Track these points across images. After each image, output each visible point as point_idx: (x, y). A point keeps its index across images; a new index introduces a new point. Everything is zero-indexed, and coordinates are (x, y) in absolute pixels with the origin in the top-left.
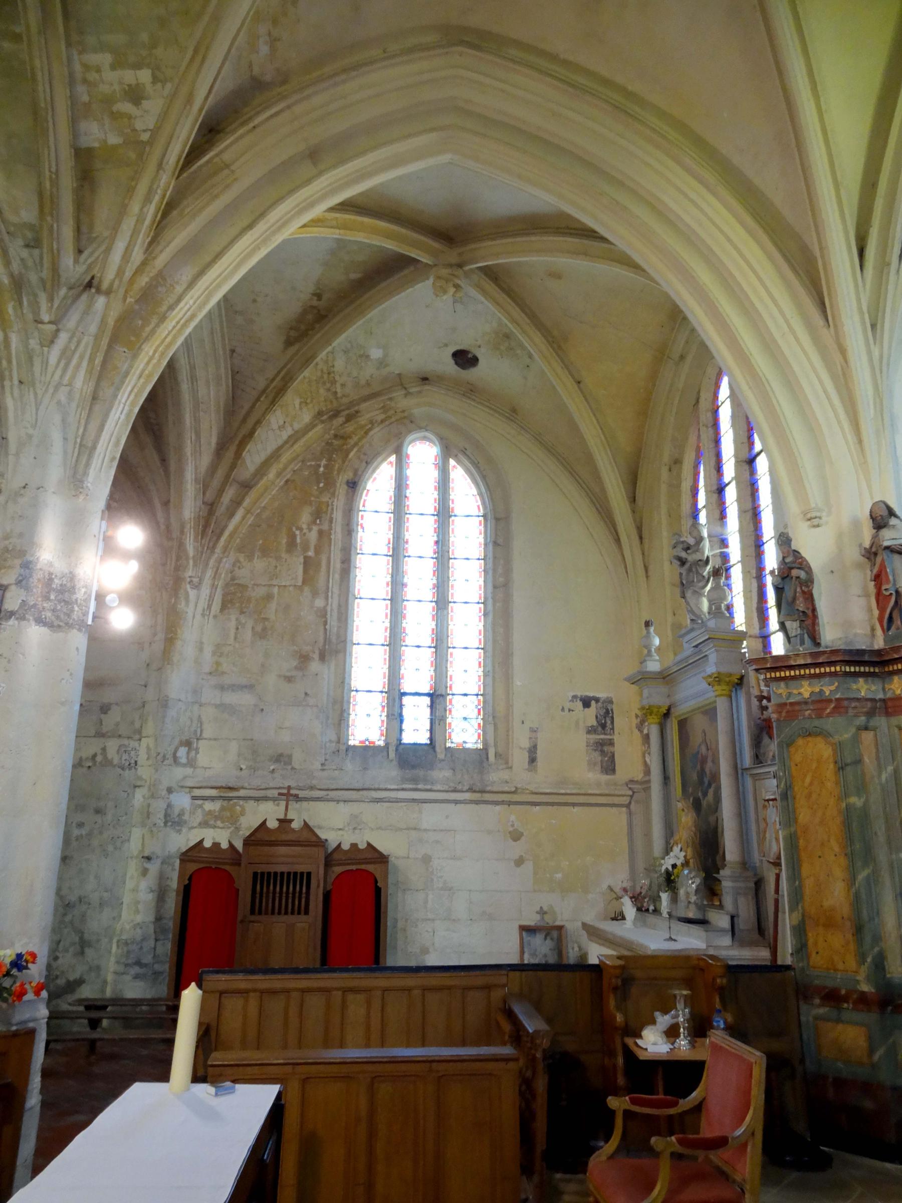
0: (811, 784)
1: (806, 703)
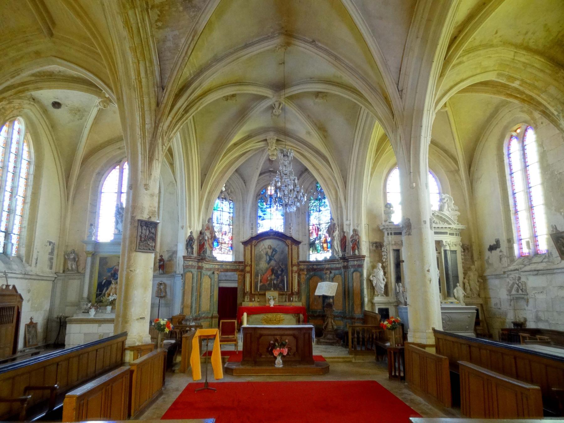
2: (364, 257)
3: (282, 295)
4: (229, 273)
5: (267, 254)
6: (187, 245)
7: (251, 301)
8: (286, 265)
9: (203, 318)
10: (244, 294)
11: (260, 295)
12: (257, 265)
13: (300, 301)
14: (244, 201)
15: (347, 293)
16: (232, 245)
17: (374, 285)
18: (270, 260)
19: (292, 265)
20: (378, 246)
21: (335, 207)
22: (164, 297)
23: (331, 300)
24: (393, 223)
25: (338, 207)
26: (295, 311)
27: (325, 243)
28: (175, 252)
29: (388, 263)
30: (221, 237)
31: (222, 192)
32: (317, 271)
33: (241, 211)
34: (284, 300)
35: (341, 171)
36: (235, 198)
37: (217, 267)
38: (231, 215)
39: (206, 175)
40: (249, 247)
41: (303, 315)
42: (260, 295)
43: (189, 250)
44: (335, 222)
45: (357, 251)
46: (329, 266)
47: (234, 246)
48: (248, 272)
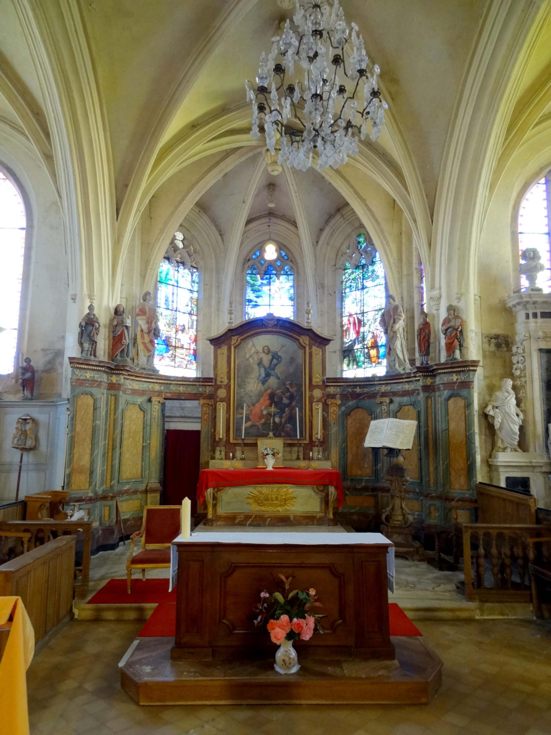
0: (83, 414)
1: (88, 380)
2: (475, 364)
3: (291, 445)
4: (189, 404)
5: (260, 363)
6: (81, 334)
7: (227, 458)
8: (300, 386)
9: (127, 492)
10: (215, 443)
11: (246, 445)
12: (239, 386)
13: (327, 458)
14: (219, 270)
15: (431, 446)
16: (195, 351)
17: (497, 425)
18: (268, 375)
19: (312, 387)
20: (501, 345)
21: (396, 275)
22: (31, 449)
23: (401, 459)
24: (540, 290)
25: (407, 271)
26: (320, 480)
27: (372, 347)
28: (59, 353)
29: (528, 379)
30: (173, 335)
31: (175, 249)
32: (362, 398)
33: (214, 288)
34: (295, 456)
35: (424, 181)
36: (202, 263)
37: (157, 388)
38: (195, 295)
39: (127, 186)
40: (224, 349)
41: (336, 488)
42: (246, 445)
43: (86, 345)
44: (397, 302)
45: (457, 352)
46: (389, 388)
47: (199, 352)
48: (222, 400)
